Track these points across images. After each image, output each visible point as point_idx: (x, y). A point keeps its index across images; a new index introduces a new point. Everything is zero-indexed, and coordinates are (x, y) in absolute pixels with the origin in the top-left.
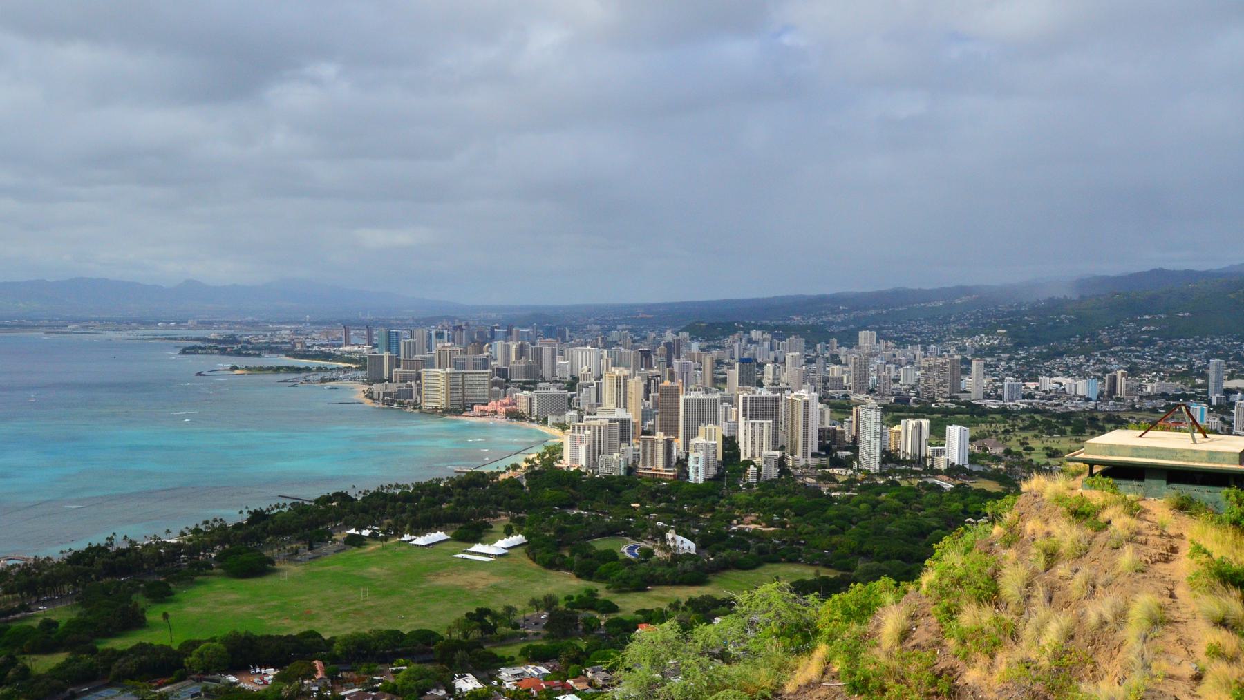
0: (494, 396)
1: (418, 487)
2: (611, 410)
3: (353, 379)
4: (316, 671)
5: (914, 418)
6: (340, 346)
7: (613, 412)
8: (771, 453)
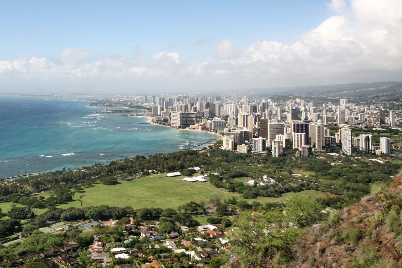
0: (197, 121)
1: (169, 154)
2: (242, 128)
3: (148, 115)
4: (131, 221)
5: (366, 134)
6: (144, 103)
7: (242, 129)
8: (305, 146)
